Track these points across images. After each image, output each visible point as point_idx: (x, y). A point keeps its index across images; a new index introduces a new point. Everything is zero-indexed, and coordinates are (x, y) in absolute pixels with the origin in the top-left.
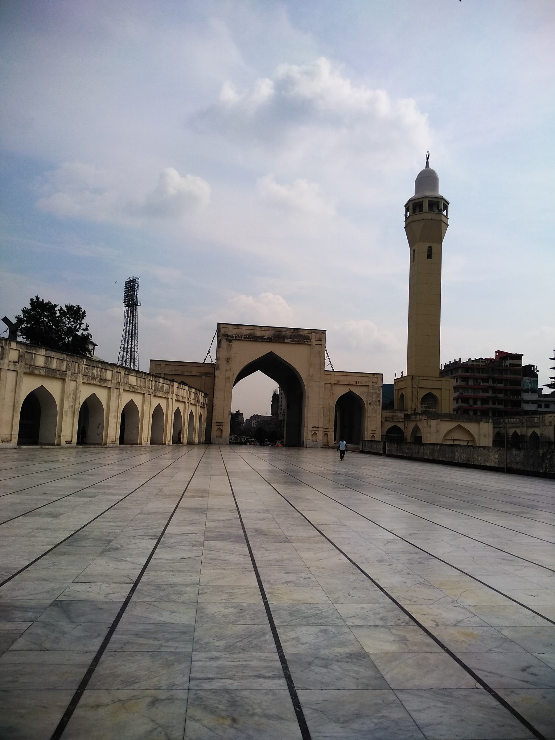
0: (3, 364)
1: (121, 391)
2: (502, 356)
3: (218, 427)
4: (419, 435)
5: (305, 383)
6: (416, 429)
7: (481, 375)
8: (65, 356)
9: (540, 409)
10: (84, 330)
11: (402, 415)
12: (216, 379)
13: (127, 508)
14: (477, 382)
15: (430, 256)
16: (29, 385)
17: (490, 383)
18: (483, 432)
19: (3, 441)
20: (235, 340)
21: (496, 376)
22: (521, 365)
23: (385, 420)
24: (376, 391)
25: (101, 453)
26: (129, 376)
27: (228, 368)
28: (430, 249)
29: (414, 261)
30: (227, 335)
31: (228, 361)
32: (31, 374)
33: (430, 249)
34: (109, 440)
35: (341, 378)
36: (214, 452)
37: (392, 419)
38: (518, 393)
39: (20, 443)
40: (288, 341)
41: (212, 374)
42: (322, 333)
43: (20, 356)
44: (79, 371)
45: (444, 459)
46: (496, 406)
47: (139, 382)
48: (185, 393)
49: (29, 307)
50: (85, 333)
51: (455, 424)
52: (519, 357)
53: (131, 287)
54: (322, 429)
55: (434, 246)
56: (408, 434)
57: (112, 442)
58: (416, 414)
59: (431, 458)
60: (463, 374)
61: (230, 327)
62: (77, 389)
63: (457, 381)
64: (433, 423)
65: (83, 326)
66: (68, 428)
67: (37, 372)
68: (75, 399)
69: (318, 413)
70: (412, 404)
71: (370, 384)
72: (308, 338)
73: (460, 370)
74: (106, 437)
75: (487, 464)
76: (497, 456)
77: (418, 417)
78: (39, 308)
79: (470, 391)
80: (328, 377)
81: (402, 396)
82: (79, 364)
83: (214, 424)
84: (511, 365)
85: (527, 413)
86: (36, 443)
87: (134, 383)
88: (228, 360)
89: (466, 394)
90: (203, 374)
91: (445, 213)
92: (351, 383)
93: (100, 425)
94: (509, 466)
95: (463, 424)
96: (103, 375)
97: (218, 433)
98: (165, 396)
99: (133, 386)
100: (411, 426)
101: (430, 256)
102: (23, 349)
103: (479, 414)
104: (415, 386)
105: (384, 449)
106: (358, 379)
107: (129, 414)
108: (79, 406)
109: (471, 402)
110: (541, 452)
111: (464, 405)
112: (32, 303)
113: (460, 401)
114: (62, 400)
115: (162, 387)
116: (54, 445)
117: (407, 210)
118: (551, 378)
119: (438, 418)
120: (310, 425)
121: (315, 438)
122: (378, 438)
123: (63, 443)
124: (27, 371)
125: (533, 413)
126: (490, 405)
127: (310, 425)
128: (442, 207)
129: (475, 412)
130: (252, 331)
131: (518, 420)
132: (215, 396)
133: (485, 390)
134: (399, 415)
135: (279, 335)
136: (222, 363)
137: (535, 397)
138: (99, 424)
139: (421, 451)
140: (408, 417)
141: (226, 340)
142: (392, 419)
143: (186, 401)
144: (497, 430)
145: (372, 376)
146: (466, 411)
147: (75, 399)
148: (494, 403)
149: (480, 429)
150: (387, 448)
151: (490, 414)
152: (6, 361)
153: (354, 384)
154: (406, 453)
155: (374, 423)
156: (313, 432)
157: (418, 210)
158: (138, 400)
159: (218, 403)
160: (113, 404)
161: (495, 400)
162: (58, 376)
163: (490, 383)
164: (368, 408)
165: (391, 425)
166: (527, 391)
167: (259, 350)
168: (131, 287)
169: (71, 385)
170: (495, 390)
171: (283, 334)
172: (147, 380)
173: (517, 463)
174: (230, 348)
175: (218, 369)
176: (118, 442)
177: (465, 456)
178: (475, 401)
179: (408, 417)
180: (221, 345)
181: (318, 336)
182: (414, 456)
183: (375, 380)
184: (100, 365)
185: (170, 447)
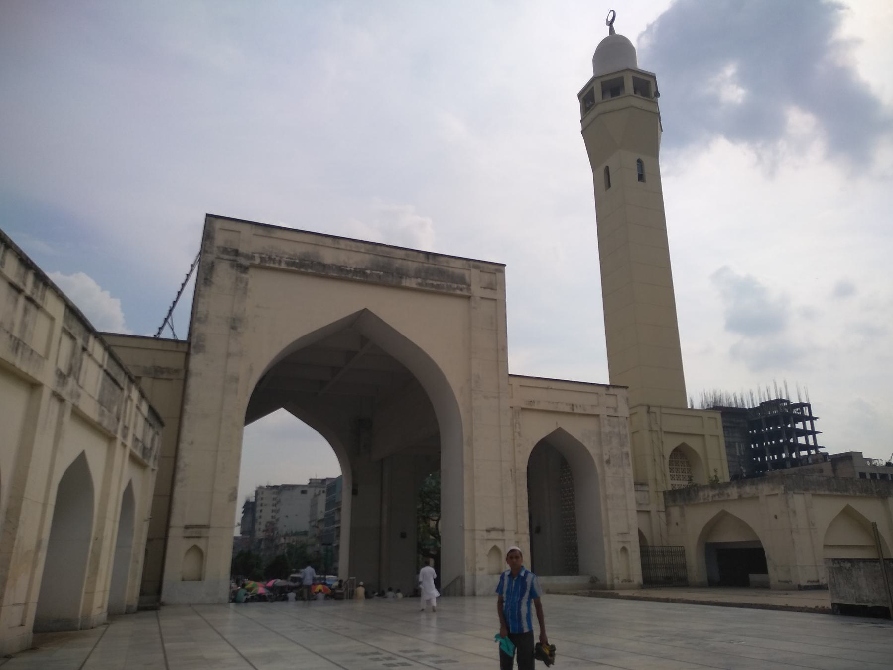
3: (192, 542)
12: (193, 382)
15: (641, 177)
20: (261, 267)
24: (616, 430)
28: (639, 161)
29: (608, 185)
30: (236, 252)
31: (233, 328)
33: (639, 161)
40: (412, 283)
41: (177, 371)
42: (499, 268)
61: (245, 230)
83: (175, 533)
88: (235, 324)
101: (641, 177)
104: (655, 428)
119: (806, 490)
130: (309, 249)
132: (186, 435)
141: (232, 266)
145: (602, 391)
153: (567, 409)
156: (490, 545)
159: (191, 458)
171: (398, 263)
175: (200, 348)
180: (216, 279)
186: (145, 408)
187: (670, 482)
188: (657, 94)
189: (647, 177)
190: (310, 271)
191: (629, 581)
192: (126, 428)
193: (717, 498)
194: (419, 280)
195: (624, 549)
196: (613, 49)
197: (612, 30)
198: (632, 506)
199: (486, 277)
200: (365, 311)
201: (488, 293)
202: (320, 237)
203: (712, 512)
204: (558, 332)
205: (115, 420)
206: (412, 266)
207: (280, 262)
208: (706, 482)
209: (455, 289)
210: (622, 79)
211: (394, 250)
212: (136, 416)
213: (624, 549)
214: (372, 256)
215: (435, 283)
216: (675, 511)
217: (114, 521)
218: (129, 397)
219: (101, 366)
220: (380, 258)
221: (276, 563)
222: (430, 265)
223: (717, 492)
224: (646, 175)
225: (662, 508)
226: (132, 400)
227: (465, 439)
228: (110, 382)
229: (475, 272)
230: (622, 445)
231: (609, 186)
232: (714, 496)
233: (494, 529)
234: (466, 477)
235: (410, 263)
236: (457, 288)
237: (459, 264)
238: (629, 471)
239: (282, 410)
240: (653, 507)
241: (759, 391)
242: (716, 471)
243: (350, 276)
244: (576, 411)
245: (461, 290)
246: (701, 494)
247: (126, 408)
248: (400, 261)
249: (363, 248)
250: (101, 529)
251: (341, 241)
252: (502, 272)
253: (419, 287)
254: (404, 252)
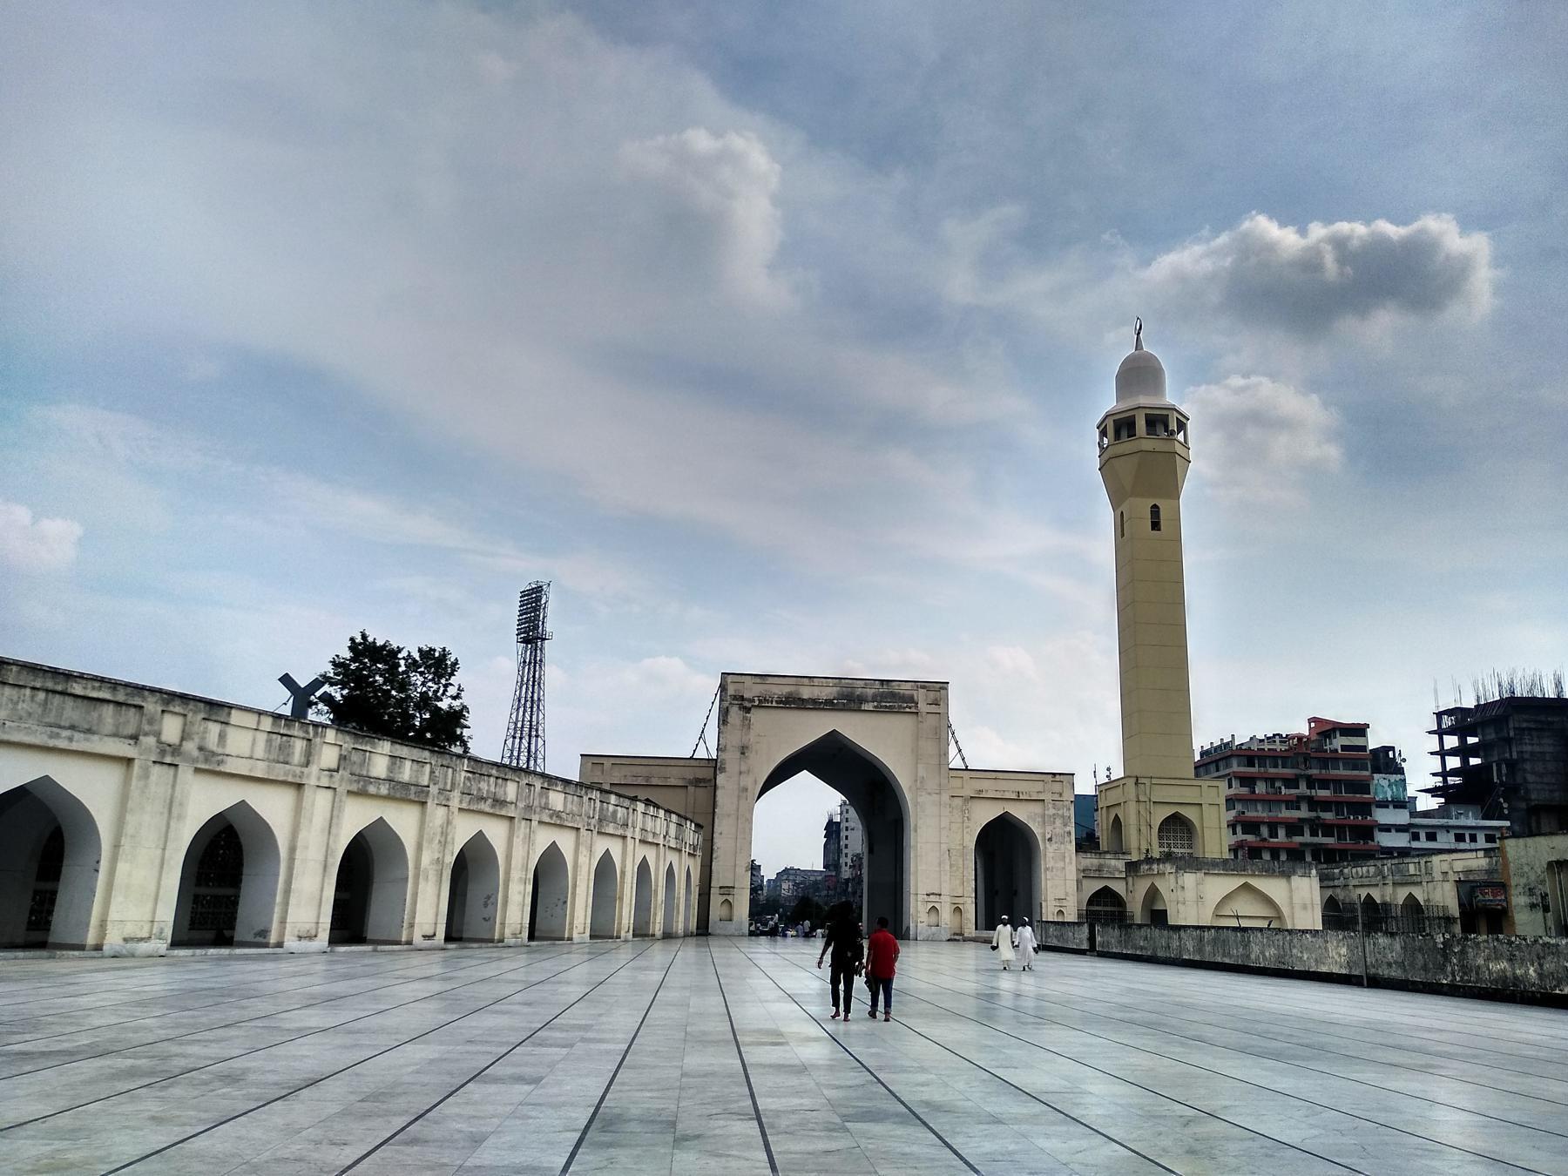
0: (309, 776)
1: (534, 823)
2: (1326, 730)
4: (1159, 907)
6: (1153, 894)
7: (1280, 770)
8: (427, 754)
9: (1415, 845)
10: (454, 698)
11: (1120, 865)
13: (645, 1067)
14: (1273, 786)
15: (1156, 525)
16: (357, 817)
17: (1303, 789)
18: (1299, 898)
19: (300, 938)
21: (1314, 772)
22: (1364, 748)
23: (1085, 874)
25: (500, 959)
26: (551, 794)
27: (744, 768)
28: (1155, 510)
30: (742, 698)
32: (361, 794)
33: (1155, 510)
34: (508, 932)
35: (985, 785)
36: (718, 950)
37: (1098, 873)
38: (1365, 808)
39: (333, 941)
40: (869, 706)
43: (342, 758)
44: (453, 784)
45: (1227, 961)
46: (1321, 839)
47: (569, 806)
48: (659, 824)
49: (348, 655)
50: (456, 703)
51: (1236, 882)
52: (1360, 730)
53: (533, 602)
54: (948, 899)
55: (1163, 505)
56: (1135, 907)
57: (514, 935)
58: (1149, 860)
59: (1197, 958)
60: (1242, 769)
62: (449, 822)
63: (1230, 786)
64: (1189, 879)
65: (452, 691)
66: (427, 905)
67: (372, 789)
68: (444, 844)
69: (939, 868)
70: (1141, 839)
71: (1047, 797)
72: (911, 699)
73: (1234, 762)
74: (503, 924)
75: (1324, 969)
76: (1344, 951)
77: (1155, 866)
78: (369, 655)
79: (1259, 807)
80: (957, 783)
81: (1117, 823)
82: (454, 771)
84: (1344, 748)
85: (1389, 852)
86: (359, 939)
87: (560, 808)
88: (743, 750)
89: (1251, 814)
90: (691, 782)
91: (1181, 437)
92: (1007, 796)
93: (489, 901)
94: (1373, 971)
95: (1254, 882)
96: (500, 796)
97: (724, 911)
98: (619, 832)
99: (557, 814)
100: (1142, 887)
101: (1156, 525)
102: (348, 743)
103: (1283, 857)
105: (1092, 939)
106: (1022, 786)
107: (548, 871)
108: (450, 859)
109: (1265, 831)
110: (1440, 939)
111: (1250, 838)
112: (353, 646)
113: (1239, 829)
114: (419, 848)
115: (615, 812)
116: (398, 943)
117: (1103, 433)
118: (1434, 774)
120: (922, 890)
121: (933, 919)
122: (1071, 916)
123: (418, 940)
124: (354, 787)
125: (1404, 853)
126: (1307, 838)
127: (922, 890)
128: (1173, 426)
129: (1275, 853)
130: (792, 689)
131: (1372, 869)
133: (1293, 804)
134: (1113, 862)
135: (850, 697)
136: (731, 757)
137: (1402, 817)
138: (489, 897)
139: (1175, 944)
140: (1132, 867)
142: (1098, 873)
143: (661, 841)
144: (1329, 892)
146: (1256, 850)
147: (444, 844)
148: (1314, 834)
149: (1291, 890)
150: (1098, 939)
151: (1309, 858)
152: (314, 769)
154: (1142, 948)
155: (1061, 883)
157: (1124, 433)
158: (566, 842)
160: (516, 853)
161: (1316, 826)
162: (412, 797)
163: (1303, 789)
165: (1097, 886)
166: (1383, 804)
167: (809, 729)
168: (533, 602)
169: (437, 815)
170: (1314, 804)
171: (858, 692)
172: (585, 799)
173: (1389, 965)
174: (747, 725)
175: (723, 770)
176: (526, 934)
177: (1273, 951)
178: (1273, 827)
179: (1132, 867)
181: (932, 694)
182: (1160, 954)
183: (1057, 787)
184: (494, 772)
185: (629, 945)
206: (870, 692)
221: (783, 910)
239: (805, 778)
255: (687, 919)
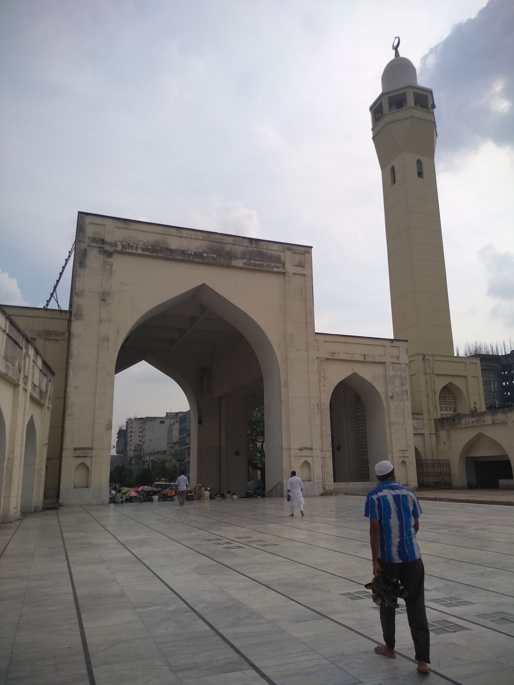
3: (80, 460)
5: (278, 352)
12: (75, 342)
15: (420, 174)
20: (122, 253)
24: (398, 373)
28: (419, 162)
30: (103, 241)
31: (104, 300)
33: (419, 162)
40: (239, 263)
41: (62, 334)
61: (110, 224)
71: (388, 360)
83: (67, 453)
88: (104, 297)
101: (420, 174)
104: (428, 371)
130: (159, 238)
132: (71, 381)
141: (100, 252)
145: (388, 343)
153: (361, 359)
156: (303, 460)
164: (389, 405)
171: (228, 248)
175: (79, 316)
186: (39, 362)
187: (440, 412)
188: (434, 106)
189: (425, 174)
190: (160, 255)
191: (408, 485)
192: (26, 377)
193: (475, 424)
194: (245, 261)
195: (404, 462)
196: (398, 69)
197: (397, 54)
198: (411, 431)
199: (297, 257)
200: (204, 285)
201: (299, 270)
202: (167, 228)
203: (472, 434)
204: (353, 299)
205: (18, 372)
206: (239, 249)
207: (137, 249)
208: (468, 412)
209: (273, 267)
210: (405, 94)
211: (224, 237)
212: (33, 368)
213: (404, 462)
214: (207, 242)
215: (257, 263)
216: (443, 434)
217: (22, 446)
218: (27, 353)
219: (4, 331)
220: (214, 244)
221: (143, 474)
222: (253, 248)
223: (476, 419)
224: (425, 172)
225: (433, 431)
226: (29, 356)
227: (282, 382)
228: (12, 343)
229: (288, 253)
230: (403, 384)
231: (395, 182)
232: (473, 422)
233: (305, 448)
234: (283, 410)
235: (237, 247)
236: (275, 266)
237: (276, 247)
238: (409, 404)
240: (426, 431)
241: (510, 342)
242: (475, 403)
243: (191, 258)
244: (367, 360)
245: (278, 267)
246: (463, 421)
247: (25, 362)
248: (230, 245)
249: (200, 236)
250: (12, 452)
251: (184, 231)
252: (310, 253)
253: (244, 266)
254: (231, 239)
255: (27, 489)
